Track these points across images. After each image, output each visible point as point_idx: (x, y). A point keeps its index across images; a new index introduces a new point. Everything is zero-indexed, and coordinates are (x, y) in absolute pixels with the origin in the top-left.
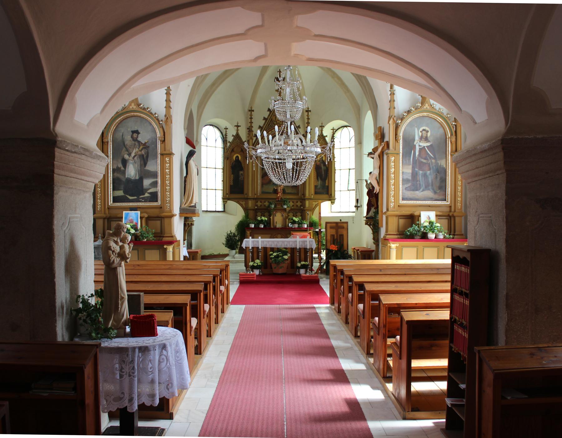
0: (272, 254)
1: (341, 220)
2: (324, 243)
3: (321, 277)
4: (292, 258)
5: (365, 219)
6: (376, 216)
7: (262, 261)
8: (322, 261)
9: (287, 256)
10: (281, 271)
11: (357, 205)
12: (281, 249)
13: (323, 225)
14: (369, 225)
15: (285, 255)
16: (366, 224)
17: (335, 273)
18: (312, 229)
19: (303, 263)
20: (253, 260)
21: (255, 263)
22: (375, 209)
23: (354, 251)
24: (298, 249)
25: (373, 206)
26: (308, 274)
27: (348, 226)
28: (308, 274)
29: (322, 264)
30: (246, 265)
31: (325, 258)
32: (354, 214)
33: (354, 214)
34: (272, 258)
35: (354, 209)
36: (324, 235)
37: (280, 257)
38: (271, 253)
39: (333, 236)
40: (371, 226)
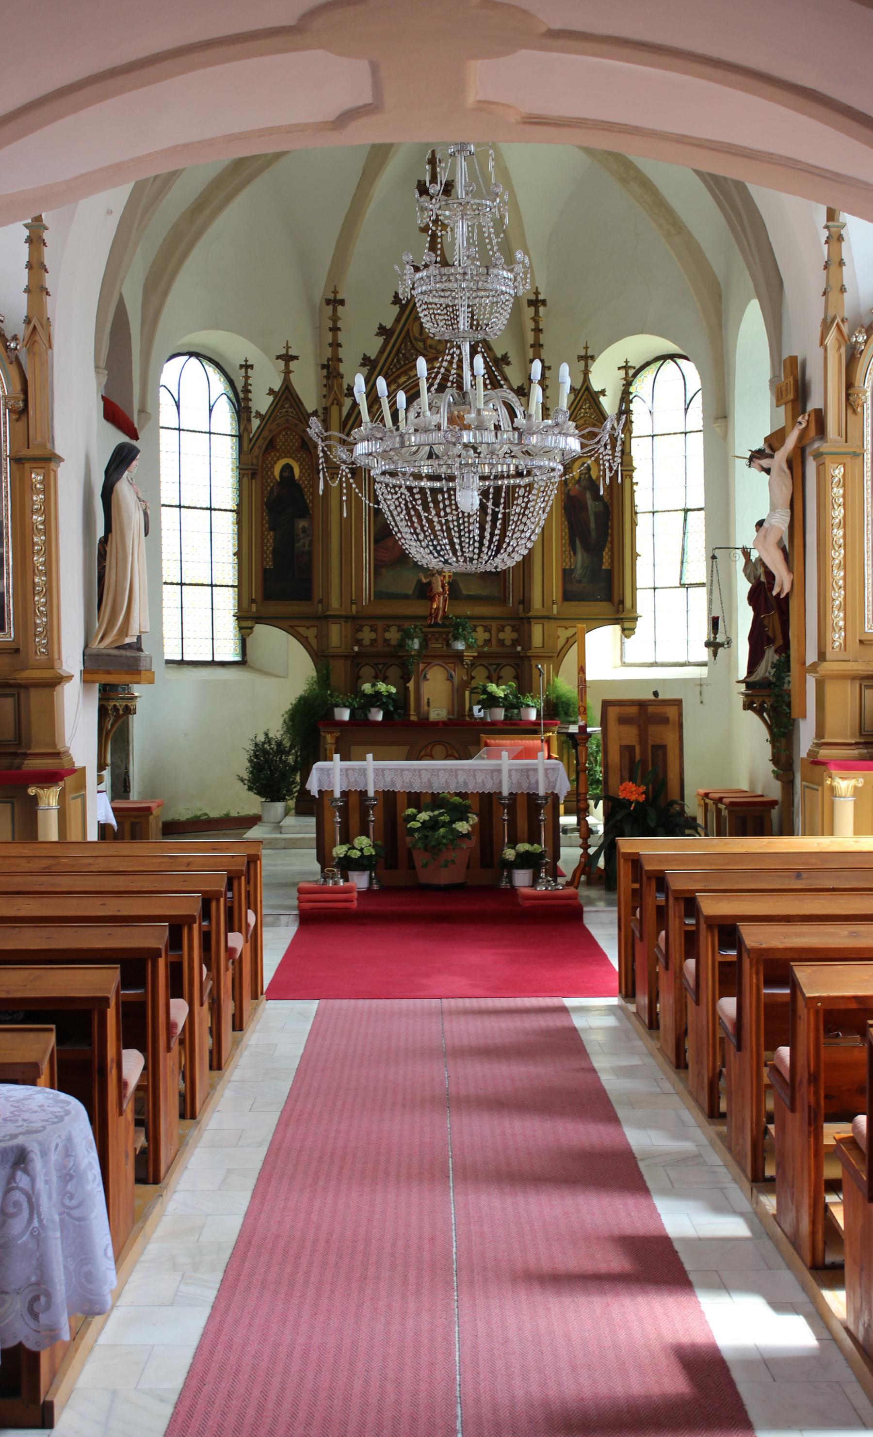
0: (413, 818)
1: (656, 694)
2: (600, 776)
3: (588, 897)
4: (485, 829)
5: (743, 688)
6: (783, 678)
7: (379, 842)
8: (590, 841)
9: (467, 822)
10: (444, 878)
11: (715, 638)
12: (443, 798)
13: (595, 712)
14: (759, 712)
15: (461, 820)
16: (748, 706)
17: (636, 886)
18: (556, 725)
19: (523, 847)
20: (346, 839)
21: (354, 848)
22: (776, 651)
23: (706, 805)
24: (505, 798)
25: (770, 641)
26: (541, 888)
27: (680, 715)
28: (541, 888)
29: (591, 851)
30: (323, 857)
31: (601, 829)
32: (703, 672)
33: (703, 672)
34: (413, 830)
35: (704, 654)
36: (597, 746)
37: (443, 826)
38: (411, 811)
39: (627, 750)
40: (765, 715)
